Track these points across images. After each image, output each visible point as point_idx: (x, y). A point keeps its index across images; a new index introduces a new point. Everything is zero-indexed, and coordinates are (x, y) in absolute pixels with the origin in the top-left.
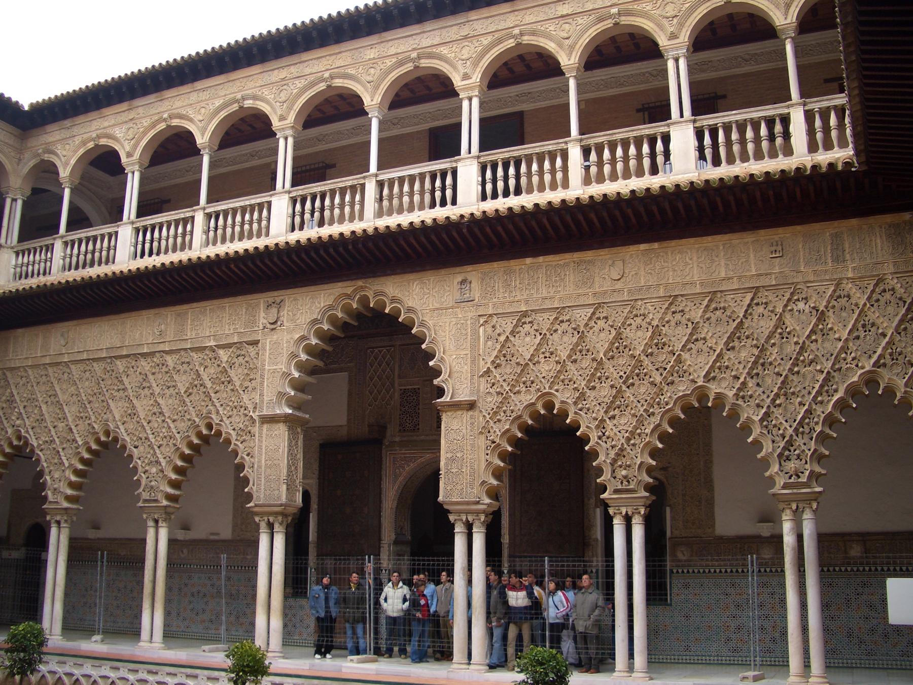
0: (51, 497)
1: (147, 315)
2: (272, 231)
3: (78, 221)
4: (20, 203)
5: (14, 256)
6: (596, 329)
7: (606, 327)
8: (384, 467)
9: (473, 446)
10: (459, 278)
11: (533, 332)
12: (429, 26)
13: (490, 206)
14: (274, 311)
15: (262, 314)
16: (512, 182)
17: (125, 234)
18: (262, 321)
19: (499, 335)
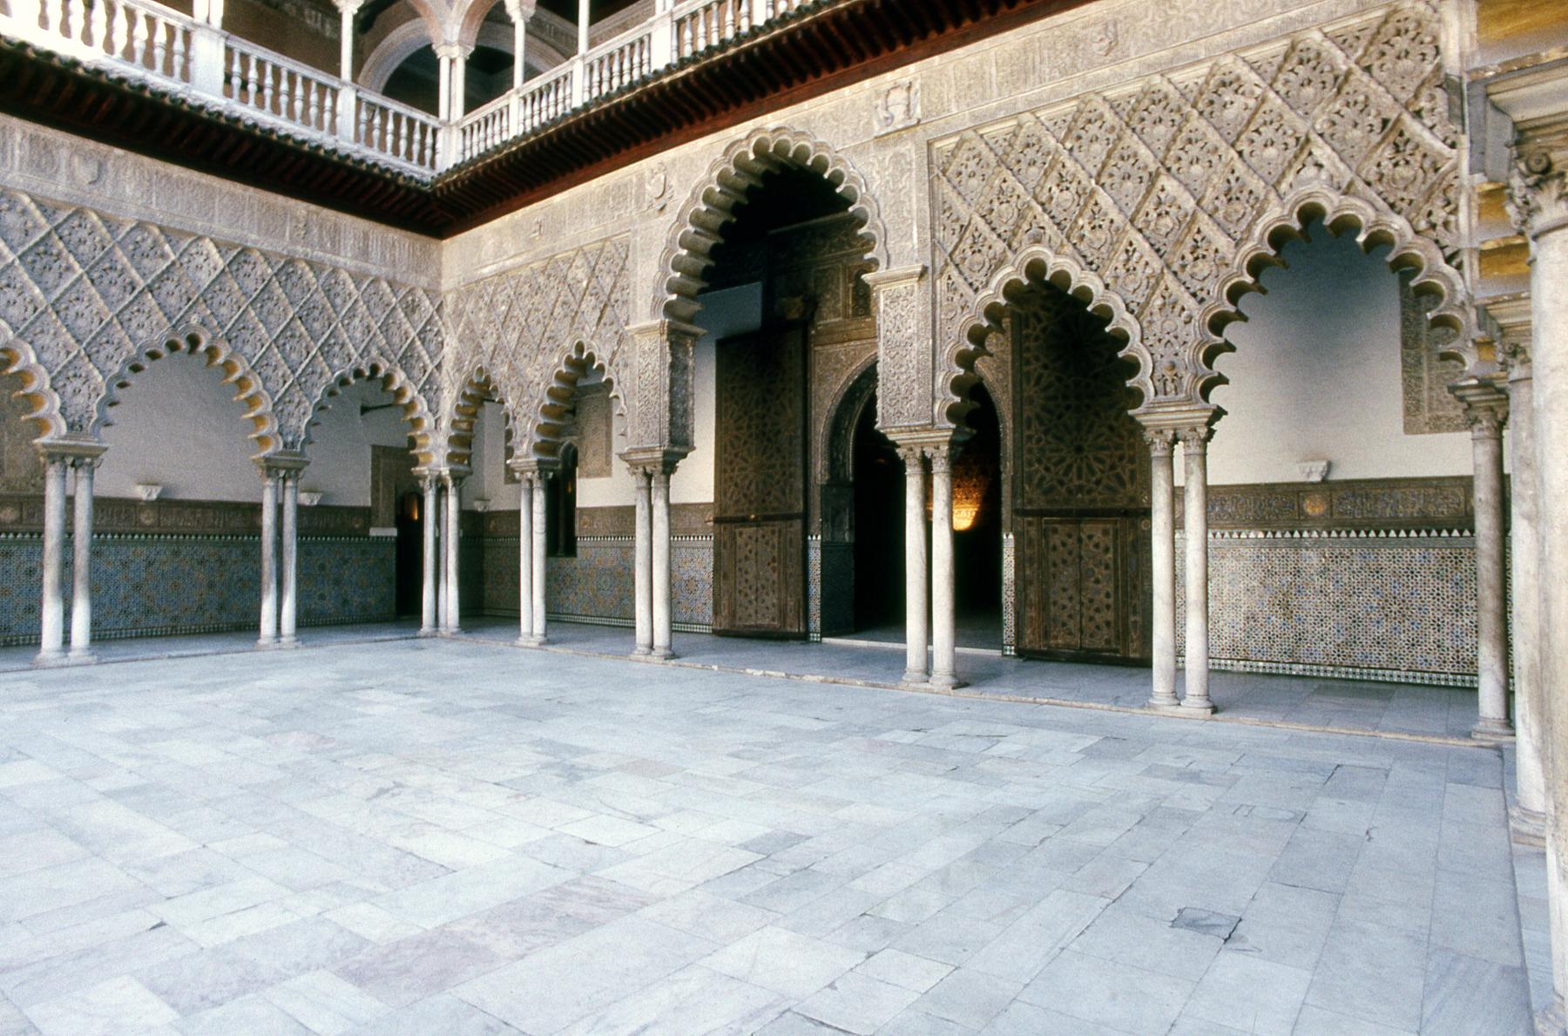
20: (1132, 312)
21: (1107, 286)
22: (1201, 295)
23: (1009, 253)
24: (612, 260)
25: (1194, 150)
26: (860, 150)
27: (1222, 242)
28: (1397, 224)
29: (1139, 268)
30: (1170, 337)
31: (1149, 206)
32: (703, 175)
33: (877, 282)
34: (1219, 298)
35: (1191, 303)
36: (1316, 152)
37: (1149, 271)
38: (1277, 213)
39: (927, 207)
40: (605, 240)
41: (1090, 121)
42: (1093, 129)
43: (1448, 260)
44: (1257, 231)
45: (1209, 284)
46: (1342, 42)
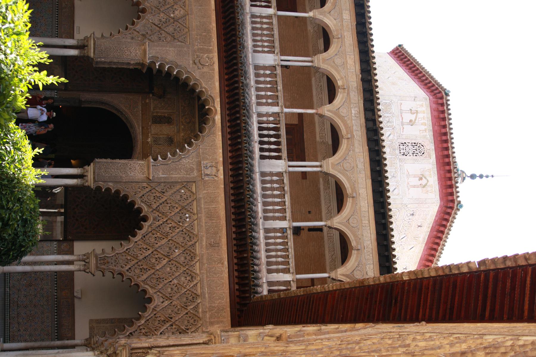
20: (127, 250)
21: (136, 242)
22: (130, 271)
23: (151, 210)
25: (174, 269)
26: (198, 155)
27: (145, 277)
28: (143, 322)
29: (141, 252)
30: (117, 262)
31: (160, 255)
32: (204, 85)
33: (149, 161)
34: (128, 275)
35: (127, 268)
36: (167, 302)
37: (139, 255)
38: (151, 291)
39: (173, 180)
40: (189, 30)
41: (190, 237)
42: (188, 238)
43: (131, 333)
44: (147, 286)
45: (133, 272)
46: (196, 308)
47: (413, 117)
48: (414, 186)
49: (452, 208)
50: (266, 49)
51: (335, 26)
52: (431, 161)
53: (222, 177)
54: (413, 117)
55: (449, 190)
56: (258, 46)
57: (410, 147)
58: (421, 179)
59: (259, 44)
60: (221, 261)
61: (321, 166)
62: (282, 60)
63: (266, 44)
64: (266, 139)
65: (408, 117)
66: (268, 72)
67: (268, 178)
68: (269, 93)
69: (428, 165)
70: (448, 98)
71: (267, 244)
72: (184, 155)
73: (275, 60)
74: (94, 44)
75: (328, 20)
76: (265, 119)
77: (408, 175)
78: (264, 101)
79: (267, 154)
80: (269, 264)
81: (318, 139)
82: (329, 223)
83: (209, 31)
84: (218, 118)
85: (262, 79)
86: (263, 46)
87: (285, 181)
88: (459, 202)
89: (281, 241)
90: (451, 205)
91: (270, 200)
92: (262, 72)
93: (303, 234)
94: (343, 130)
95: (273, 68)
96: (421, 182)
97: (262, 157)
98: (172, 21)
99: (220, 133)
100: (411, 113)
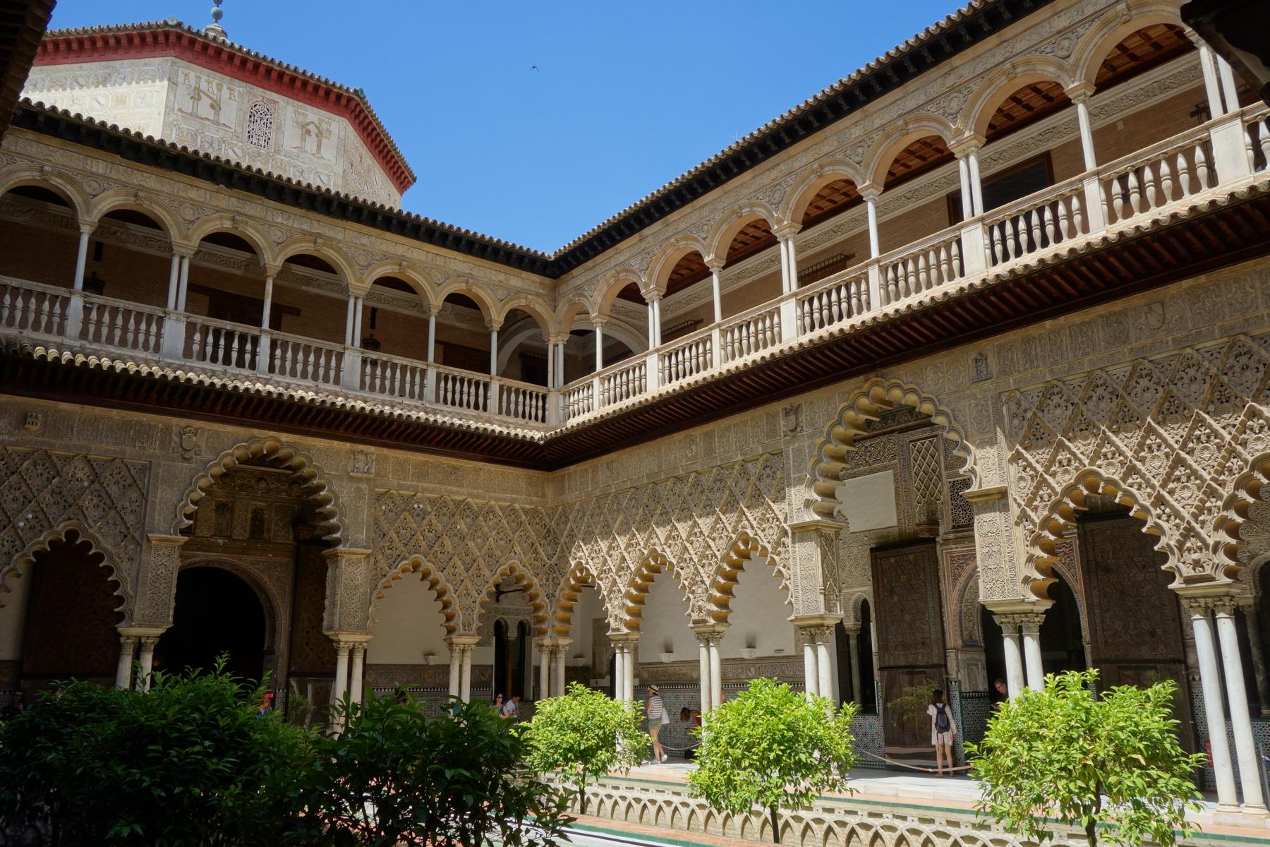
0: (613, 624)
1: (679, 436)
2: (784, 337)
3: (616, 352)
4: (561, 348)
5: (561, 397)
6: (1139, 389)
7: (1151, 385)
8: (941, 567)
9: (1009, 538)
10: (974, 355)
11: (1063, 404)
12: (911, 85)
13: (1002, 269)
14: (793, 417)
15: (782, 422)
16: (1023, 238)
17: (653, 362)
18: (783, 429)
19: (1025, 411)
24: (139, 480)
27: (487, 573)
28: (535, 580)
46: (526, 512)
47: (206, 102)
48: (319, 147)
49: (358, 105)
50: (154, 328)
51: (116, 195)
52: (281, 103)
53: (373, 449)
54: (206, 102)
55: (333, 97)
56: (146, 341)
57: (255, 126)
58: (308, 132)
59: (141, 338)
60: (478, 470)
61: (356, 298)
62: (176, 308)
63: (143, 326)
64: (310, 369)
65: (204, 109)
66: (197, 337)
67: (368, 379)
68: (236, 345)
69: (290, 113)
70: (186, 27)
71: (453, 403)
72: (337, 498)
73: (178, 320)
74: (141, 626)
75: (104, 203)
76: (277, 362)
77: (301, 149)
78: (248, 357)
79: (332, 373)
80: (476, 407)
81: (239, 272)
82: (434, 311)
83: (127, 425)
84: (284, 437)
85: (209, 350)
86: (148, 333)
87: (375, 357)
88: (356, 92)
89: (450, 383)
90: (353, 105)
91: (397, 384)
92: (196, 347)
93: (378, 336)
94: (305, 248)
95: (191, 329)
96: (313, 135)
97: (337, 381)
98: (96, 486)
99: (310, 439)
100: (199, 99)
